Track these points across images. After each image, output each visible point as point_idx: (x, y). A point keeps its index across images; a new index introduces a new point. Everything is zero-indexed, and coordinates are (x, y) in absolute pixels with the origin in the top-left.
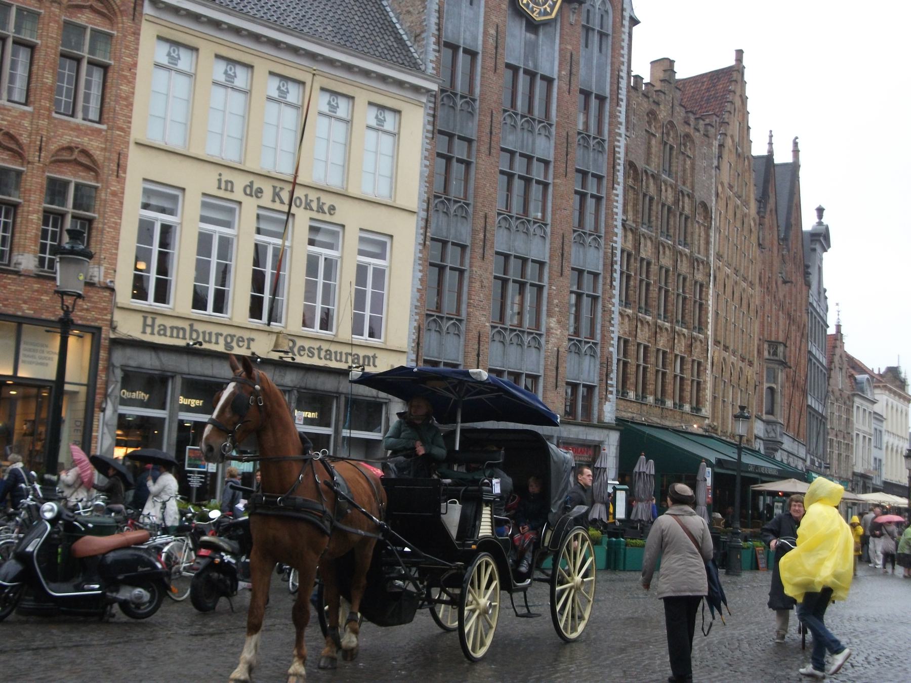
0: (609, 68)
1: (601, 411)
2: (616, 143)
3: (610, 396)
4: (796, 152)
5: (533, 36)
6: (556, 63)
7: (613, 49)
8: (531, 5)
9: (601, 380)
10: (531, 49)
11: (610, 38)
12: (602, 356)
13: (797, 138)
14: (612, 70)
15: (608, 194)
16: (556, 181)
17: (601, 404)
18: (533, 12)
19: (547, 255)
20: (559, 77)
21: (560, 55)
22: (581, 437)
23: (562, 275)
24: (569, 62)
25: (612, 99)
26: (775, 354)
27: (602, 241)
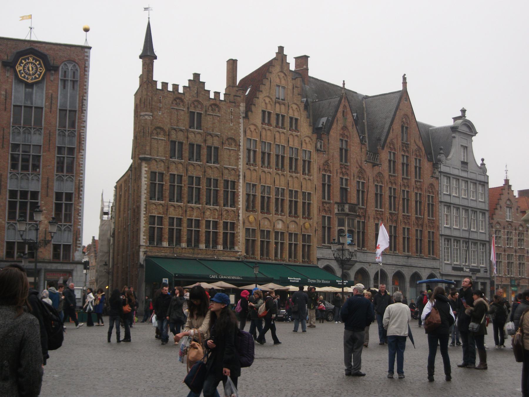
0: (78, 96)
1: (73, 255)
2: (82, 131)
3: (78, 249)
4: (405, 83)
5: (30, 90)
6: (44, 100)
7: (80, 88)
8: (27, 76)
9: (73, 241)
10: (29, 96)
11: (78, 83)
12: (74, 230)
13: (405, 75)
14: (79, 97)
15: (77, 156)
16: (45, 154)
17: (73, 253)
18: (28, 79)
19: (40, 188)
20: (46, 106)
21: (46, 96)
22: (59, 268)
23: (47, 196)
24: (51, 99)
25: (79, 111)
26: (343, 210)
27: (74, 178)
